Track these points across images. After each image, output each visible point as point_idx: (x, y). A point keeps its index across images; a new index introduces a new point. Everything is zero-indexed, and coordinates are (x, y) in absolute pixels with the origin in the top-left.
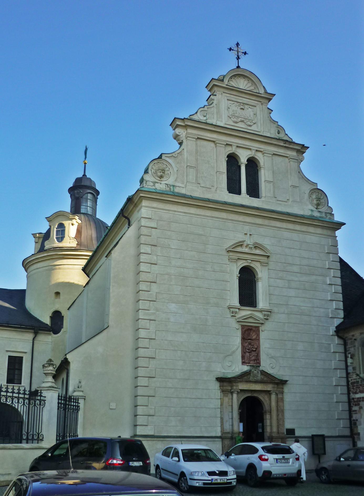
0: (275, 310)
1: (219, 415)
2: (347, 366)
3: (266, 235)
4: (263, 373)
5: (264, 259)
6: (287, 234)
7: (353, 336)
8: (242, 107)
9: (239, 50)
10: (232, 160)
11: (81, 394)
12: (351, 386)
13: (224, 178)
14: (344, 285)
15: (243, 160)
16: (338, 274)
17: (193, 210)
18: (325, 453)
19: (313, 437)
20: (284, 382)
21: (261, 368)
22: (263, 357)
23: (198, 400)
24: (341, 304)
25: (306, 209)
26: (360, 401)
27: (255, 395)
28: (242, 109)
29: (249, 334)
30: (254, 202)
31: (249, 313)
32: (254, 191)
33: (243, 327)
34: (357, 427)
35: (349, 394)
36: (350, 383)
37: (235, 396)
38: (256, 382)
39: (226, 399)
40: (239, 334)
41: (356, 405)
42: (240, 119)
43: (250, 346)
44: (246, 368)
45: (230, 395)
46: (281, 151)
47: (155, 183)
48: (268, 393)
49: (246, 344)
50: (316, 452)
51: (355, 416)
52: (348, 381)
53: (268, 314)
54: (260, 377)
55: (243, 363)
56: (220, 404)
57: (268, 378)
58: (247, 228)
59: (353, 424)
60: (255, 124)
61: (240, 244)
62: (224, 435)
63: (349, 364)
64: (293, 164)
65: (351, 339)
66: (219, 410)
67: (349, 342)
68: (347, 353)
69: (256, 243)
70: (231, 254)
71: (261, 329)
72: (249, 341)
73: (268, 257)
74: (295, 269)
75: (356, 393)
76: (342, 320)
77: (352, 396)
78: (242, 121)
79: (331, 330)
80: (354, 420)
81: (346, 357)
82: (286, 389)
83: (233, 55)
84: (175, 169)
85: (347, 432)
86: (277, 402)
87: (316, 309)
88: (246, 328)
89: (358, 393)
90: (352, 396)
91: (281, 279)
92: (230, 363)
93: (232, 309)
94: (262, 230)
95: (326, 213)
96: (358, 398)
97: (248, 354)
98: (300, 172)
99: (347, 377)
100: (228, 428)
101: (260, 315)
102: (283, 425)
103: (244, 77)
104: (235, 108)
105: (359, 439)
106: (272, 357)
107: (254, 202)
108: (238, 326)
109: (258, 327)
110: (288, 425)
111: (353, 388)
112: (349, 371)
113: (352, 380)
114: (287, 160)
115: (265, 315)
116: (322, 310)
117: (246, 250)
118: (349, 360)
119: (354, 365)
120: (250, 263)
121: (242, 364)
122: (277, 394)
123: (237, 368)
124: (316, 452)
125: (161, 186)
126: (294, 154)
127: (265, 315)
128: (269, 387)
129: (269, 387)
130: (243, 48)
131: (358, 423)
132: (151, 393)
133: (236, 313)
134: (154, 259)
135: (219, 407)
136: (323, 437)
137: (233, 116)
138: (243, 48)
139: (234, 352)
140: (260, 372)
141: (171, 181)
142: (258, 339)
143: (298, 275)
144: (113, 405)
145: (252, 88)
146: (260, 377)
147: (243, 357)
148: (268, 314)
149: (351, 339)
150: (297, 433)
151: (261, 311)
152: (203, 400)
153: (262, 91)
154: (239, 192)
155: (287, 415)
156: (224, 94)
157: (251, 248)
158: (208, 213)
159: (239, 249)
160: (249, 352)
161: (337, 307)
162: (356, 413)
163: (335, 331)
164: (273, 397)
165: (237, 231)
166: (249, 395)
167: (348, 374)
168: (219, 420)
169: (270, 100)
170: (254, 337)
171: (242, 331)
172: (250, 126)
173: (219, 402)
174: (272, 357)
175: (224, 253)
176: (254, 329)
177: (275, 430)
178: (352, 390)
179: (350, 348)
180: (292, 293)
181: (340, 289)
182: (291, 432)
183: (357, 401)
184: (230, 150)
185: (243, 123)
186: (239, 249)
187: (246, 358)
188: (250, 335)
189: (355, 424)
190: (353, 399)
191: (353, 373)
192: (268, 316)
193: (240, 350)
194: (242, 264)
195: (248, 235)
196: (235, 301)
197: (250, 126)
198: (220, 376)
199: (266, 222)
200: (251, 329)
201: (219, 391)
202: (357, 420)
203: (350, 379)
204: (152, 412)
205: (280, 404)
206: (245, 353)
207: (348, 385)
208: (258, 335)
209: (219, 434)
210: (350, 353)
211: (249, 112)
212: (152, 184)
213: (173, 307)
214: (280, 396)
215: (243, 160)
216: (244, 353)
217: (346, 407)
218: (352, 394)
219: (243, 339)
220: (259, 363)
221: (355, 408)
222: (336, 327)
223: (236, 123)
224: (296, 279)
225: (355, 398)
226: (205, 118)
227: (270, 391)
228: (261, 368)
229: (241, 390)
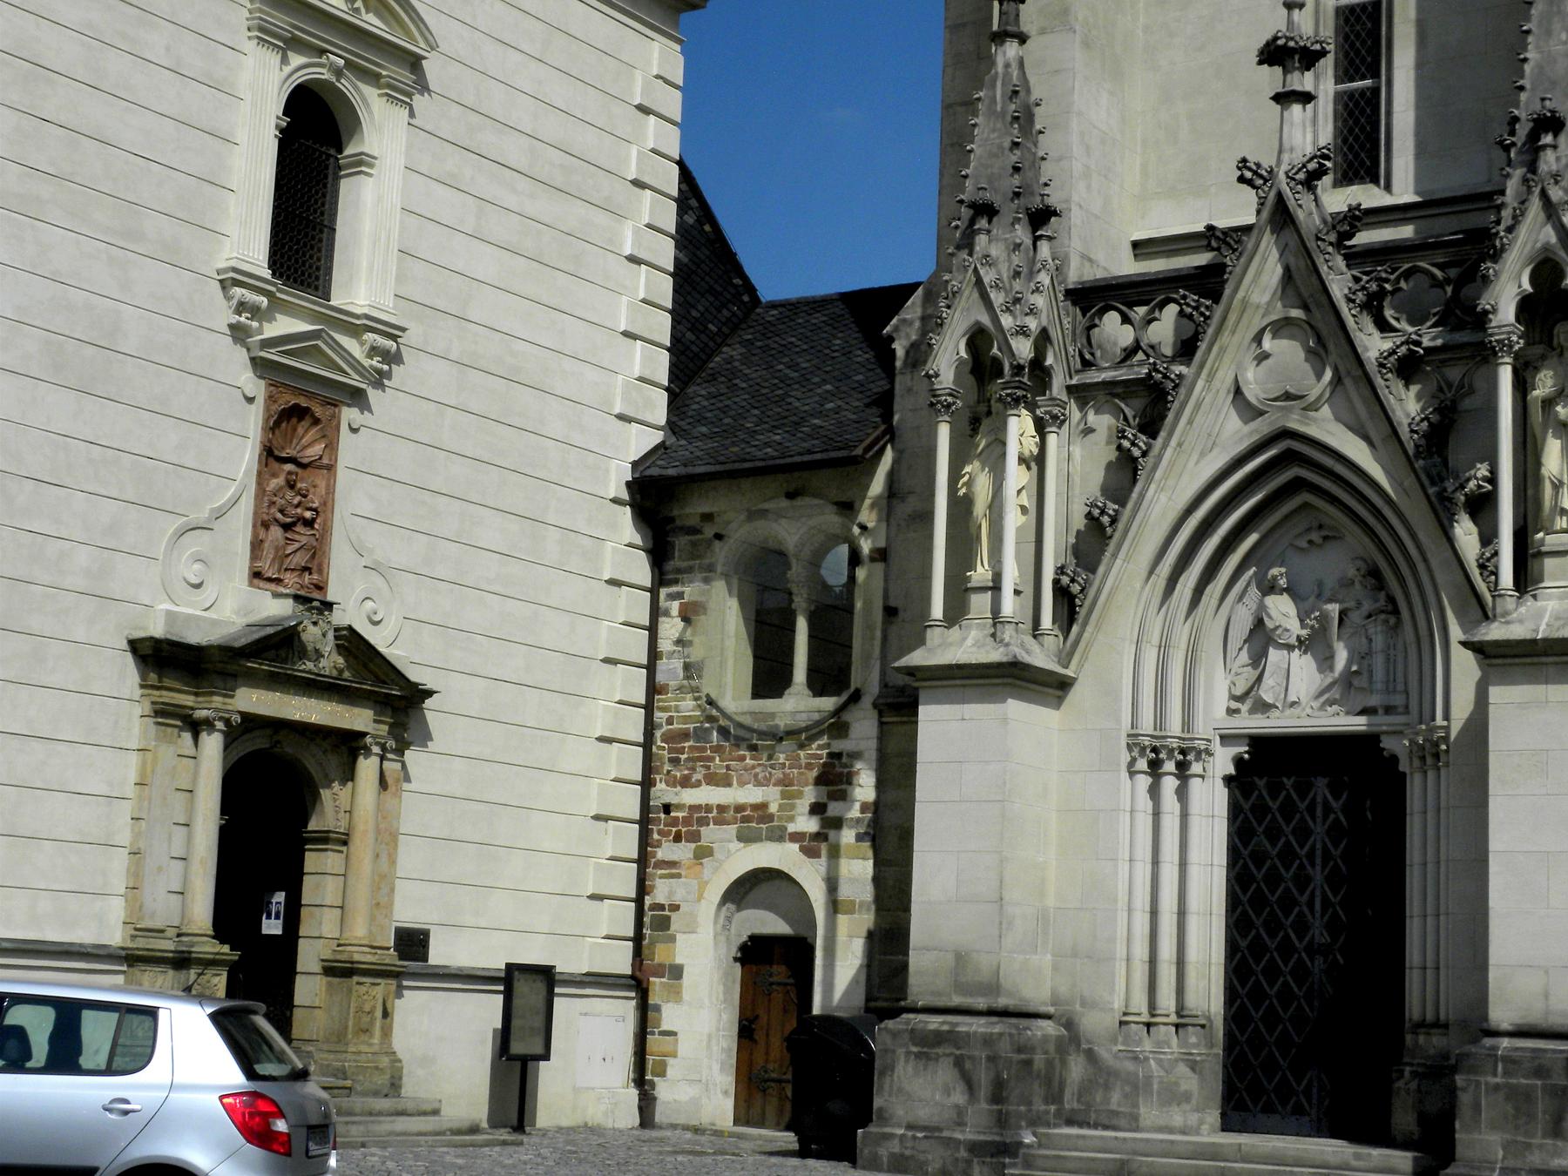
1: (124, 837)
2: (654, 654)
4: (353, 644)
5: (391, 71)
7: (708, 517)
12: (660, 747)
14: (683, 276)
16: (669, 220)
19: (510, 979)
21: (339, 618)
23: (34, 743)
24: (664, 358)
26: (703, 822)
27: (290, 748)
34: (673, 939)
35: (646, 784)
36: (658, 734)
37: (212, 744)
39: (167, 753)
40: (253, 422)
41: (678, 838)
43: (289, 494)
44: (274, 608)
45: (187, 736)
48: (349, 745)
49: (276, 483)
50: (517, 1048)
51: (661, 891)
52: (650, 727)
55: (256, 575)
56: (133, 777)
59: (649, 923)
62: (141, 943)
63: (665, 645)
65: (694, 531)
66: (126, 810)
67: (681, 542)
68: (663, 592)
72: (289, 467)
74: (514, 150)
75: (685, 783)
76: (657, 437)
77: (663, 792)
79: (613, 476)
80: (661, 907)
81: (656, 612)
85: (620, 960)
87: (568, 364)
89: (698, 784)
90: (663, 792)
92: (197, 566)
93: (238, 292)
96: (694, 808)
97: (276, 532)
99: (649, 708)
100: (162, 910)
105: (676, 994)
110: (408, 914)
111: (675, 761)
112: (660, 678)
113: (670, 721)
116: (591, 374)
118: (671, 628)
119: (696, 653)
120: (338, 73)
121: (251, 584)
124: (517, 1048)
127: (374, 351)
128: (358, 718)
129: (358, 718)
131: (676, 920)
133: (255, 312)
135: (130, 791)
136: (546, 976)
139: (220, 514)
140: (331, 635)
143: (523, 183)
146: (331, 662)
147: (256, 546)
149: (694, 531)
150: (438, 955)
152: (62, 747)
155: (410, 858)
160: (287, 527)
161: (647, 375)
162: (679, 876)
163: (628, 484)
164: (367, 768)
167: (653, 689)
168: (119, 863)
170: (317, 449)
171: (267, 409)
176: (318, 410)
178: (667, 767)
179: (679, 571)
180: (487, 263)
181: (665, 289)
182: (413, 943)
183: (687, 821)
187: (268, 552)
189: (663, 924)
190: (667, 808)
191: (680, 688)
193: (246, 507)
198: (157, 630)
201: (138, 710)
202: (675, 908)
203: (660, 716)
206: (266, 525)
207: (647, 744)
208: (332, 446)
209: (115, 937)
210: (672, 597)
216: (262, 524)
217: (627, 840)
218: (661, 786)
219: (270, 454)
221: (666, 851)
222: (635, 464)
224: (511, 201)
225: (679, 807)
227: (364, 734)
228: (339, 618)
229: (247, 717)
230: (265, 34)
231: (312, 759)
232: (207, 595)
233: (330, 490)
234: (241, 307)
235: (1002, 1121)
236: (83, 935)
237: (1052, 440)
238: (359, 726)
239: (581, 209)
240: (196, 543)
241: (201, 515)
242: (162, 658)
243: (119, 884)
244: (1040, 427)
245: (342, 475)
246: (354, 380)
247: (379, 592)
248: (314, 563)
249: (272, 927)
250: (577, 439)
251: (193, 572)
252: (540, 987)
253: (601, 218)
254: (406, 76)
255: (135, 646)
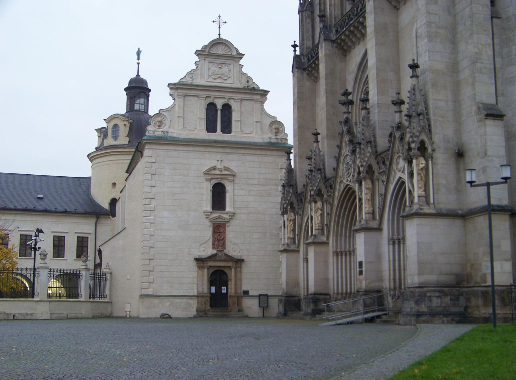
0: (238, 211)
1: (196, 282)
3: (233, 162)
4: (226, 255)
6: (249, 158)
8: (220, 66)
9: (221, 21)
10: (211, 107)
11: (108, 270)
13: (204, 123)
15: (219, 107)
17: (180, 148)
18: (268, 306)
19: (260, 295)
20: (242, 261)
21: (225, 251)
22: (228, 244)
25: (267, 137)
27: (221, 269)
28: (220, 68)
29: (219, 229)
30: (226, 137)
31: (218, 215)
32: (227, 128)
33: (214, 224)
37: (206, 270)
38: (220, 261)
39: (200, 272)
40: (211, 229)
42: (218, 76)
44: (215, 252)
46: (248, 97)
47: (154, 132)
48: (229, 267)
49: (216, 236)
53: (233, 215)
54: (223, 258)
55: (213, 248)
57: (229, 258)
58: (219, 156)
60: (229, 77)
61: (214, 168)
64: (258, 105)
66: (196, 279)
69: (225, 167)
70: (206, 176)
71: (227, 225)
73: (234, 175)
74: (255, 182)
78: (220, 77)
82: (243, 265)
83: (216, 25)
84: (169, 119)
86: (236, 273)
88: (216, 225)
91: (243, 189)
94: (230, 157)
95: (281, 139)
97: (217, 242)
98: (263, 110)
100: (201, 290)
101: (226, 216)
102: (241, 288)
103: (222, 43)
104: (214, 68)
106: (234, 244)
107: (226, 137)
108: (210, 224)
109: (225, 225)
110: (245, 288)
114: (253, 102)
115: (229, 216)
116: (274, 210)
117: (217, 172)
122: (235, 269)
123: (210, 251)
125: (159, 133)
126: (259, 97)
128: (230, 264)
129: (230, 264)
130: (223, 19)
132: (151, 269)
133: (209, 215)
134: (153, 183)
136: (267, 295)
137: (213, 74)
138: (223, 19)
139: (207, 241)
141: (165, 128)
142: (224, 232)
144: (129, 277)
145: (228, 50)
147: (213, 244)
148: (233, 215)
150: (251, 293)
151: (227, 213)
153: (234, 53)
154: (214, 130)
155: (244, 281)
156: (207, 59)
157: (221, 171)
158: (191, 149)
159: (213, 172)
164: (233, 270)
165: (211, 160)
166: (217, 269)
168: (195, 285)
169: (241, 58)
172: (226, 80)
173: (196, 274)
174: (234, 244)
175: (202, 175)
177: (233, 291)
182: (246, 293)
184: (209, 101)
185: (220, 79)
186: (213, 172)
188: (219, 230)
192: (232, 216)
194: (214, 182)
195: (220, 161)
196: (209, 209)
197: (226, 80)
198: (197, 257)
199: (234, 151)
200: (220, 226)
204: (151, 281)
205: (239, 274)
208: (225, 229)
209: (196, 294)
211: (225, 70)
212: (152, 132)
213: (166, 213)
214: (239, 269)
215: (219, 107)
216: (214, 241)
219: (214, 232)
220: (225, 248)
223: (215, 79)
224: (255, 189)
226: (191, 80)
230: (207, 180)
231: (226, 270)
232: (206, 252)
233: (225, 235)
234: (206, 215)
235: (285, 310)
236: (192, 294)
237: (297, 216)
238: (230, 265)
239: (269, 187)
240: (203, 246)
241: (203, 242)
242: (199, 261)
243: (196, 288)
244: (295, 215)
245: (227, 233)
246: (227, 220)
247: (234, 247)
248: (224, 245)
249: (224, 291)
250: (272, 219)
251: (203, 249)
252: (266, 297)
253: (274, 187)
254: (232, 178)
255: (195, 259)
